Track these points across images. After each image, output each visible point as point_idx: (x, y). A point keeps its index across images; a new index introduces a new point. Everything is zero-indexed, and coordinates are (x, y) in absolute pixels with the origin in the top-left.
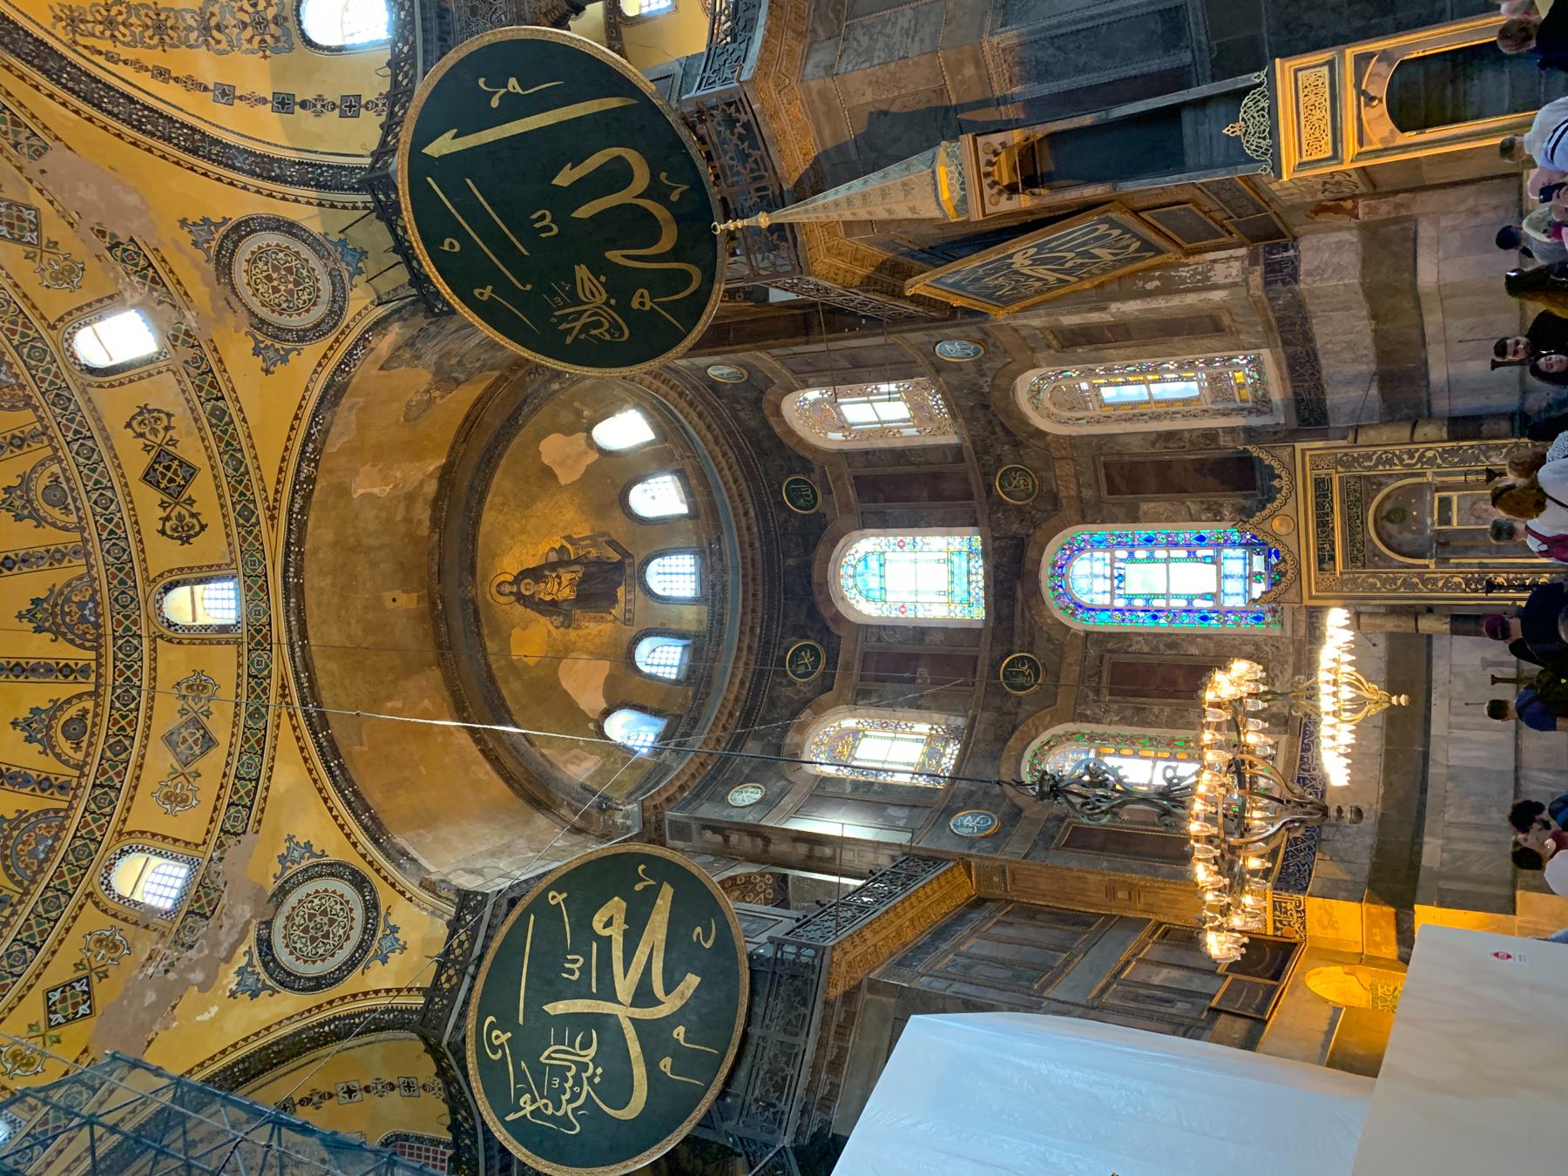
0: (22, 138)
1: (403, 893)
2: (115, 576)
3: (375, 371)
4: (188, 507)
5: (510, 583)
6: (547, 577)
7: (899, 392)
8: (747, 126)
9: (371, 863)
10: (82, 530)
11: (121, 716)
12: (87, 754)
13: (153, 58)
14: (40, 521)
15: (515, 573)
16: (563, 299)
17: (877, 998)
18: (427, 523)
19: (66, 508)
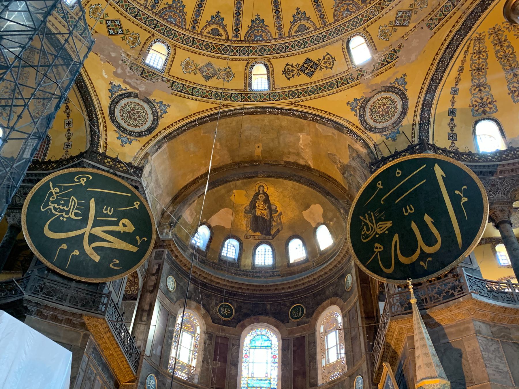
0: (434, 21)
1: (144, 146)
2: (271, 47)
3: (348, 143)
5: (263, 191)
6: (265, 205)
8: (453, 295)
9: (157, 135)
10: (289, 37)
12: (205, 36)
13: (467, 66)
14: (293, 23)
15: (267, 193)
16: (378, 216)
17: (81, 337)
18: (288, 160)
19: (297, 32)
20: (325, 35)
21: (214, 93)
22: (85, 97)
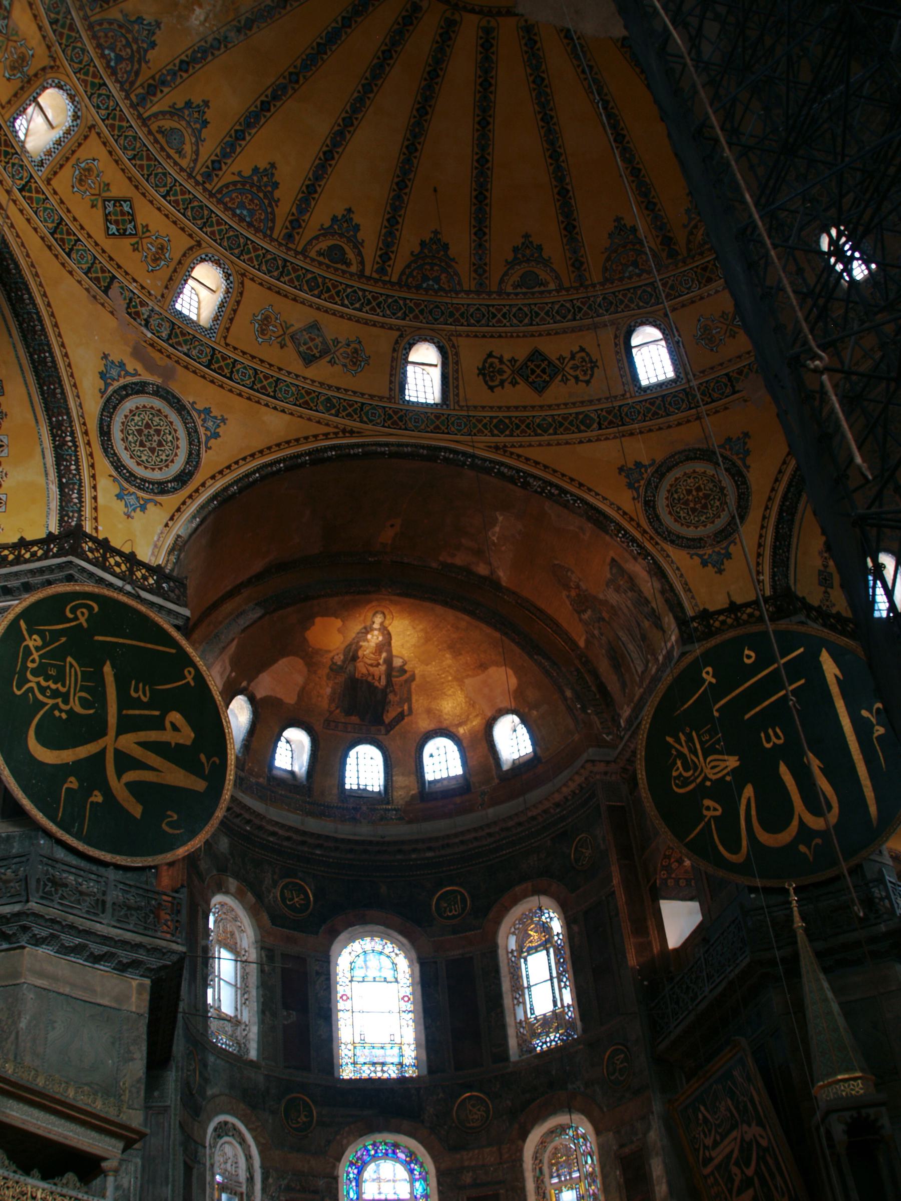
1: (172, 519)
3: (612, 554)
4: (509, 380)
5: (382, 624)
7: (563, 1006)
9: (197, 491)
10: (500, 293)
11: (340, 291)
12: (313, 260)
15: (390, 628)
16: (707, 741)
18: (449, 561)
19: (518, 285)
20: (578, 307)
21: (323, 398)
22: (49, 388)
